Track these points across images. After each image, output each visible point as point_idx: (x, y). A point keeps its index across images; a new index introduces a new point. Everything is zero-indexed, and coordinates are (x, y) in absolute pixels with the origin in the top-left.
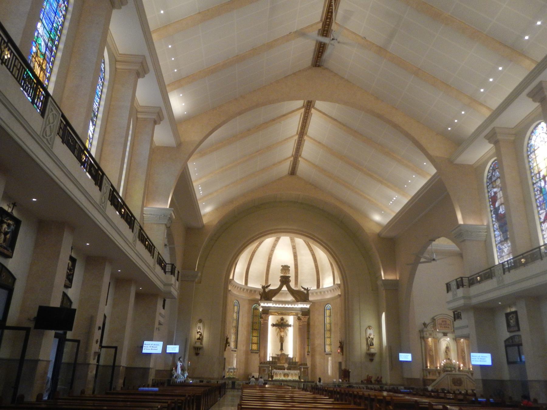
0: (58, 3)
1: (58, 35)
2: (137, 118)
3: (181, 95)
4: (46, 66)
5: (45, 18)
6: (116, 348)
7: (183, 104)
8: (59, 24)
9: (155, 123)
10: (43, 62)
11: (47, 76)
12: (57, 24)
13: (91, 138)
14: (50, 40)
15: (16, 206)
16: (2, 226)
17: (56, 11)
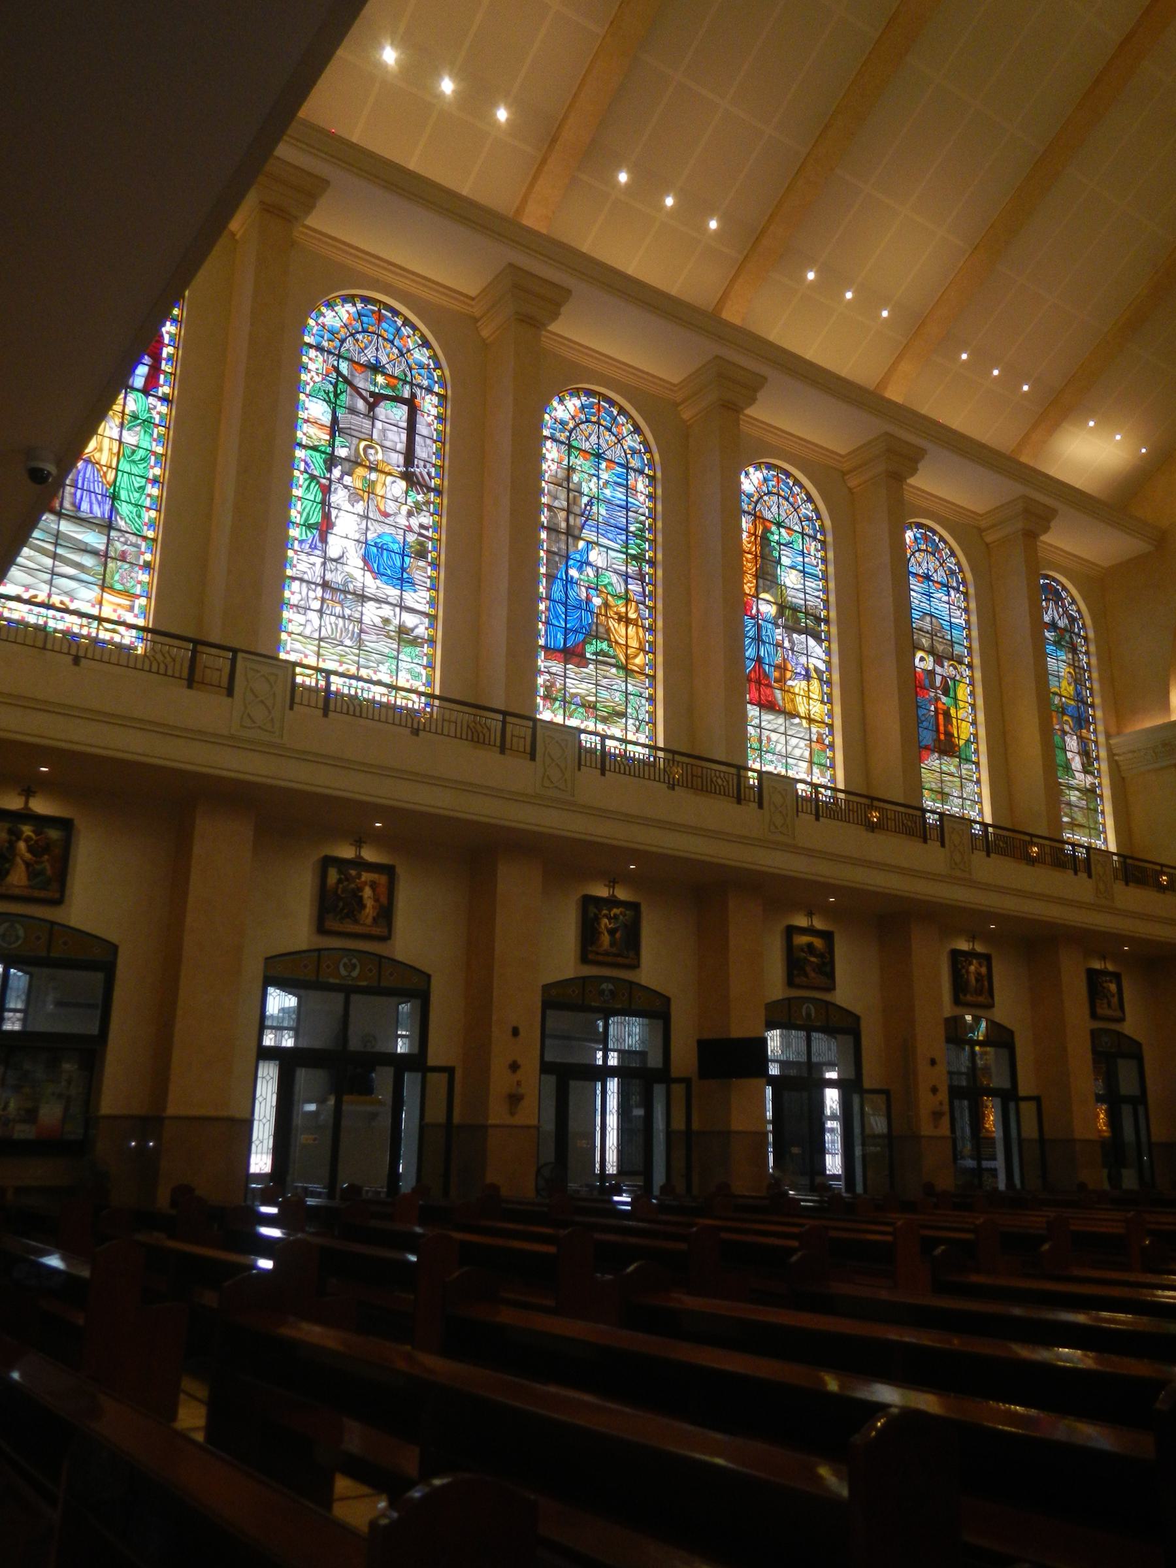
0: (627, 486)
1: (647, 540)
2: (987, 545)
3: (1091, 424)
4: (637, 610)
5: (603, 532)
6: (1037, 1099)
7: (1118, 437)
8: (643, 518)
9: (1031, 536)
10: (627, 609)
11: (647, 626)
12: (637, 523)
13: (824, 670)
14: (629, 561)
15: (618, 883)
16: (599, 924)
17: (627, 502)
